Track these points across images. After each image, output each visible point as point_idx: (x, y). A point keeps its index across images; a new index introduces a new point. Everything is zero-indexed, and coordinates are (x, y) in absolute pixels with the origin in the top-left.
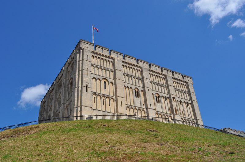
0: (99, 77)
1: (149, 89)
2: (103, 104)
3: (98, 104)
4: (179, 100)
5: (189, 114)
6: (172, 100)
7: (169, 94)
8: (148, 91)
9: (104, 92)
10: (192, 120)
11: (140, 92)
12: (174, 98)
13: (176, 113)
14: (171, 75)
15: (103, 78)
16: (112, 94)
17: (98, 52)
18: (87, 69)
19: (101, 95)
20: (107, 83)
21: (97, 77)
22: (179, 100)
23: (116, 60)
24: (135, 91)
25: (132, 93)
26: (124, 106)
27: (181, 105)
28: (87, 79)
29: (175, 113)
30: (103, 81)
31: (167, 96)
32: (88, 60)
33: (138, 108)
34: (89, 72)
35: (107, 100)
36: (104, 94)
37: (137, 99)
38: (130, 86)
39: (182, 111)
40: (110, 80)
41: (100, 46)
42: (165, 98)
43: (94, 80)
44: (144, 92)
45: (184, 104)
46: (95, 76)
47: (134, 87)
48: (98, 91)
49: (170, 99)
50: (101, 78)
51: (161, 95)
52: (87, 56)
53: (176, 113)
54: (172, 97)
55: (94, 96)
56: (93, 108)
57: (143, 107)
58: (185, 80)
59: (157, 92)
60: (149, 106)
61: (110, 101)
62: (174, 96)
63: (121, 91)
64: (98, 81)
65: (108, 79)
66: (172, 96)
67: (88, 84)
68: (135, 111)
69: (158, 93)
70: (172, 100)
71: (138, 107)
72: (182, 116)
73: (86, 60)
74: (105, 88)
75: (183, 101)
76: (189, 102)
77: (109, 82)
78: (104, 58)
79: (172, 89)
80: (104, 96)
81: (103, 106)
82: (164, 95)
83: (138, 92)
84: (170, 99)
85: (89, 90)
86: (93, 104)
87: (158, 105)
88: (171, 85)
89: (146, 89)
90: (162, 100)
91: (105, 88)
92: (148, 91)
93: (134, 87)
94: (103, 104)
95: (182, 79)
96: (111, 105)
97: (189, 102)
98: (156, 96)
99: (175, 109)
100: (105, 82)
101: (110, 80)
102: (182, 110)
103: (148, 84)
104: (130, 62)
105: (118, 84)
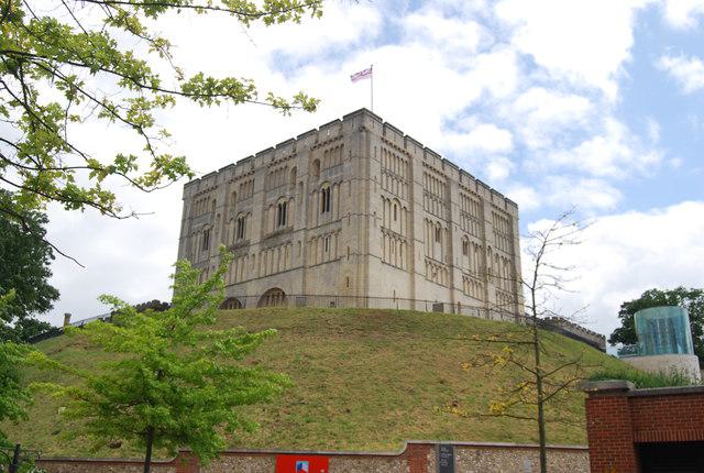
7: (484, 239)
9: (395, 228)
21: (387, 195)
23: (414, 161)
25: (432, 232)
35: (399, 243)
37: (438, 245)
38: (430, 217)
42: (476, 246)
44: (449, 231)
49: (483, 249)
50: (391, 198)
51: (472, 239)
63: (420, 231)
66: (488, 244)
76: (509, 257)
79: (488, 228)
80: (394, 234)
81: (393, 255)
82: (477, 241)
84: (483, 249)
93: (435, 220)
95: (503, 208)
97: (509, 257)
103: (456, 217)
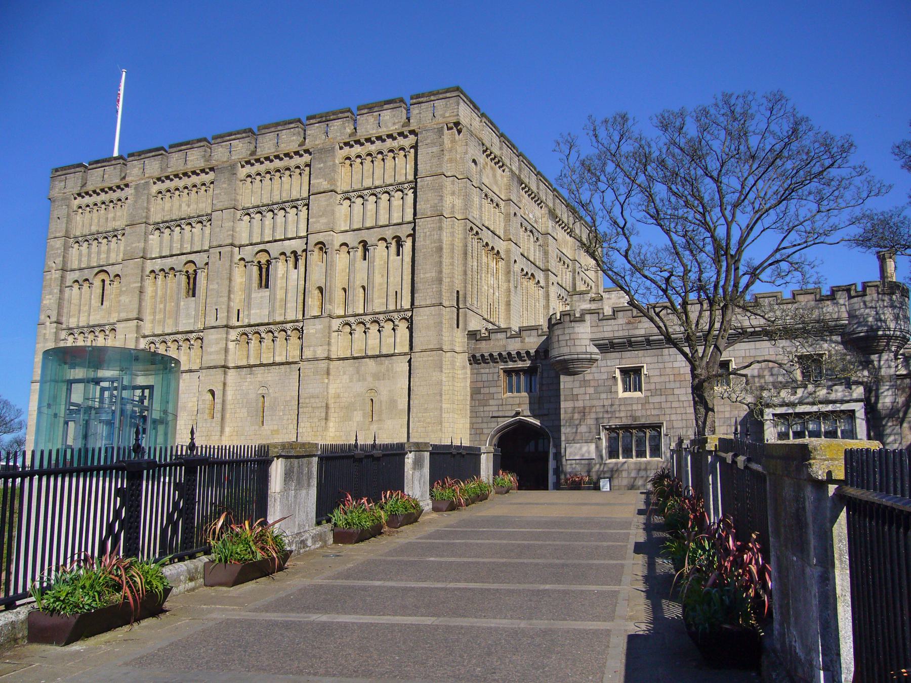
0: (87, 274)
12: (321, 246)
15: (97, 270)
28: (50, 299)
30: (97, 283)
31: (298, 245)
40: (112, 270)
59: (262, 247)
62: (320, 237)
64: (86, 285)
69: (268, 247)
75: (371, 237)
77: (112, 276)
87: (266, 293)
88: (325, 185)
90: (280, 269)
100: (103, 281)
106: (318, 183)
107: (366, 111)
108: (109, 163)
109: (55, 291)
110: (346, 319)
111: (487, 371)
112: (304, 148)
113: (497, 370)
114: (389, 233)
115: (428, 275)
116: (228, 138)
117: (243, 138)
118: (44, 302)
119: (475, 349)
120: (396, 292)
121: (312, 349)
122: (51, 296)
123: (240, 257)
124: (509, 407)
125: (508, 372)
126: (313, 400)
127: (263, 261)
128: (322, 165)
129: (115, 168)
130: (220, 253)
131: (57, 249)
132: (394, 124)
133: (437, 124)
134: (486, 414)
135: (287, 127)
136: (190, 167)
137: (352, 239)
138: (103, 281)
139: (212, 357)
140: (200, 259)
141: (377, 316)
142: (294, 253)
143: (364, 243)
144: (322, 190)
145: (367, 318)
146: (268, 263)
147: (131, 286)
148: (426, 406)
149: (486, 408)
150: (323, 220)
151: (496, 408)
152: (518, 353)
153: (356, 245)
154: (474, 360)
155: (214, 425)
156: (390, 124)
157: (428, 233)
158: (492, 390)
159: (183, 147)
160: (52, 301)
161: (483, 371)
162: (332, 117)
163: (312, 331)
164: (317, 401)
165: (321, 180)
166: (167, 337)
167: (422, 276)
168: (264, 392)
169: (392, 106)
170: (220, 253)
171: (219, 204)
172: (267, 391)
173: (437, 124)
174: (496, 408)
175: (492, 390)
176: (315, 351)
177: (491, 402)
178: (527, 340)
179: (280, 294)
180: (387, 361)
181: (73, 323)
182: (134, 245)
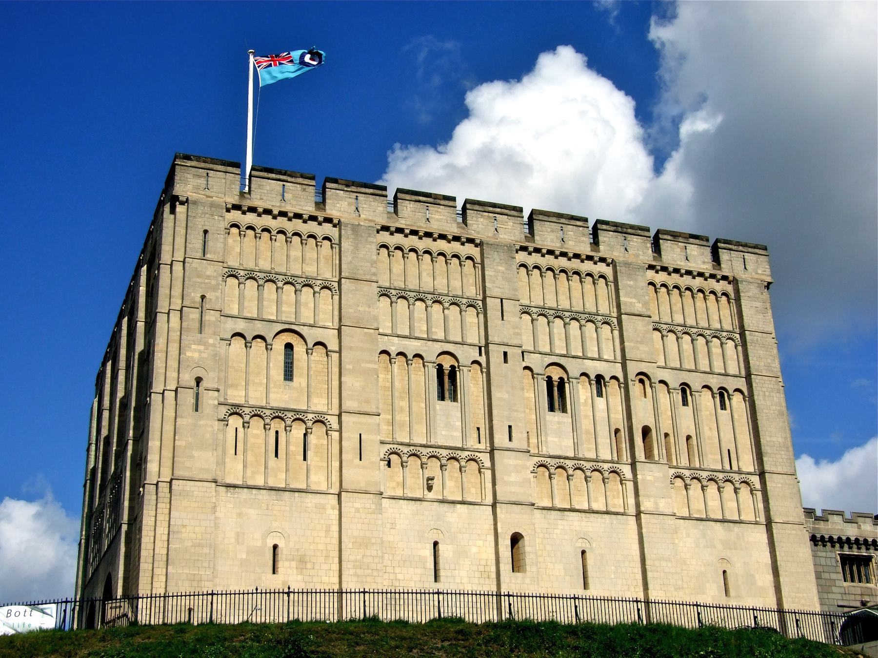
0: (259, 328)
1: (510, 351)
2: (277, 455)
3: (250, 458)
4: (674, 381)
5: (728, 443)
6: (636, 389)
8: (506, 361)
10: (736, 477)
11: (465, 369)
12: (643, 377)
13: (649, 454)
14: (647, 255)
16: (319, 404)
17: (261, 205)
18: (203, 297)
19: (268, 412)
20: (299, 349)
22: (674, 383)
24: (440, 369)
26: (375, 452)
27: (685, 403)
28: (200, 352)
29: (640, 454)
30: (279, 346)
31: (607, 370)
32: (208, 256)
33: (444, 452)
34: (210, 317)
35: (298, 431)
36: (282, 405)
38: (412, 347)
39: (688, 438)
40: (312, 335)
41: (270, 171)
43: (238, 343)
45: (706, 401)
46: (240, 326)
47: (431, 351)
48: (256, 398)
51: (574, 368)
52: (206, 232)
53: (649, 454)
54: (631, 375)
55: (235, 422)
56: (230, 480)
57: (472, 443)
58: (726, 270)
60: (501, 438)
61: (311, 438)
62: (643, 368)
64: (259, 345)
65: (304, 331)
66: (633, 369)
67: (200, 373)
68: (433, 467)
69: (562, 361)
70: (636, 389)
71: (446, 448)
72: (684, 462)
73: (199, 254)
74: (289, 375)
75: (696, 381)
77: (310, 345)
78: (291, 226)
80: (279, 415)
83: (453, 371)
85: (209, 400)
86: (227, 460)
87: (556, 418)
88: (638, 308)
89: (496, 354)
91: (289, 375)
92: (506, 361)
94: (277, 455)
96: (310, 454)
98: (549, 380)
99: (646, 431)
100: (289, 347)
101: (312, 335)
102: (687, 426)
104: (423, 227)
105: (351, 348)
106: (631, 303)
107: (669, 237)
108: (293, 180)
109: (211, 341)
110: (679, 470)
111: (824, 554)
112: (601, 254)
113: (833, 555)
114: (715, 382)
115: (774, 439)
116: (491, 209)
117: (514, 216)
118: (189, 354)
119: (814, 528)
120: (729, 450)
121: (652, 500)
122: (202, 348)
123: (524, 364)
124: (852, 597)
125: (846, 560)
126: (664, 564)
127: (555, 378)
128: (632, 283)
129: (304, 190)
130: (505, 354)
131: (208, 277)
132: (704, 263)
133: (751, 278)
134: (831, 602)
135: (573, 222)
136: (435, 227)
137: (674, 381)
138: (289, 347)
139: (512, 489)
140: (466, 355)
141: (715, 474)
142: (599, 378)
143: (685, 388)
144: (637, 313)
145: (705, 474)
146: (562, 382)
147: (363, 365)
148: (798, 585)
149: (831, 596)
150: (644, 348)
151: (839, 596)
152: (857, 540)
153: (677, 385)
154: (816, 540)
155: (528, 581)
156: (700, 262)
157: (767, 394)
158: (834, 576)
159: (421, 198)
160: (205, 355)
161: (820, 554)
162: (629, 231)
163: (649, 478)
164: (669, 564)
165: (634, 300)
166: (422, 450)
167: (768, 439)
168: (584, 545)
169: (697, 241)
170: (505, 354)
171: (496, 290)
172: (588, 545)
173: (751, 278)
174: (839, 596)
175: (834, 576)
176: (656, 503)
177: (834, 589)
178: (863, 527)
179: (586, 424)
180: (736, 528)
181: (236, 396)
182: (360, 308)
